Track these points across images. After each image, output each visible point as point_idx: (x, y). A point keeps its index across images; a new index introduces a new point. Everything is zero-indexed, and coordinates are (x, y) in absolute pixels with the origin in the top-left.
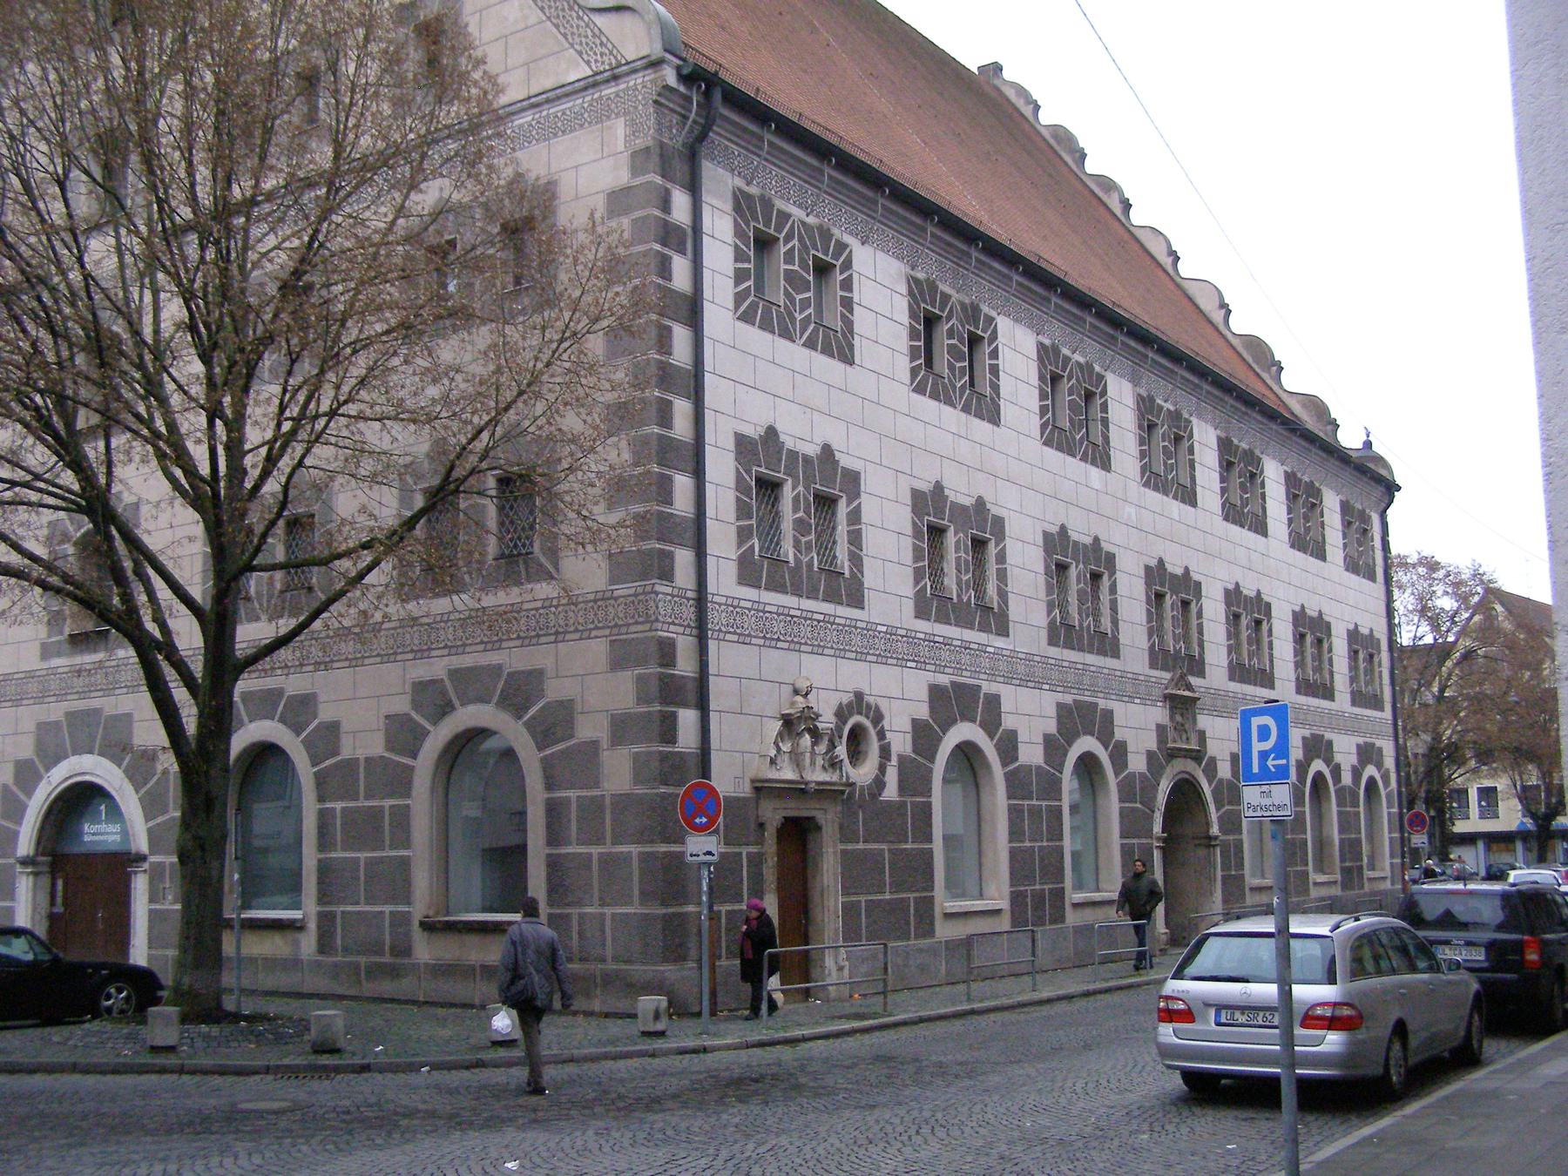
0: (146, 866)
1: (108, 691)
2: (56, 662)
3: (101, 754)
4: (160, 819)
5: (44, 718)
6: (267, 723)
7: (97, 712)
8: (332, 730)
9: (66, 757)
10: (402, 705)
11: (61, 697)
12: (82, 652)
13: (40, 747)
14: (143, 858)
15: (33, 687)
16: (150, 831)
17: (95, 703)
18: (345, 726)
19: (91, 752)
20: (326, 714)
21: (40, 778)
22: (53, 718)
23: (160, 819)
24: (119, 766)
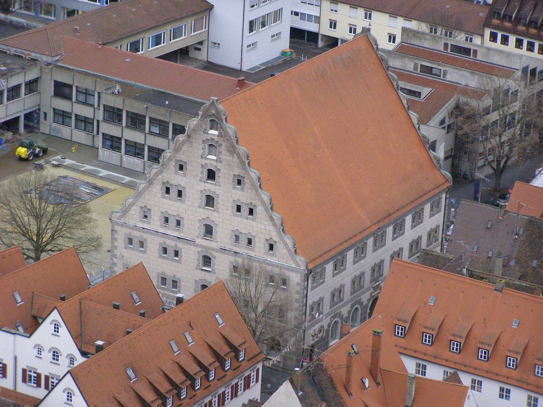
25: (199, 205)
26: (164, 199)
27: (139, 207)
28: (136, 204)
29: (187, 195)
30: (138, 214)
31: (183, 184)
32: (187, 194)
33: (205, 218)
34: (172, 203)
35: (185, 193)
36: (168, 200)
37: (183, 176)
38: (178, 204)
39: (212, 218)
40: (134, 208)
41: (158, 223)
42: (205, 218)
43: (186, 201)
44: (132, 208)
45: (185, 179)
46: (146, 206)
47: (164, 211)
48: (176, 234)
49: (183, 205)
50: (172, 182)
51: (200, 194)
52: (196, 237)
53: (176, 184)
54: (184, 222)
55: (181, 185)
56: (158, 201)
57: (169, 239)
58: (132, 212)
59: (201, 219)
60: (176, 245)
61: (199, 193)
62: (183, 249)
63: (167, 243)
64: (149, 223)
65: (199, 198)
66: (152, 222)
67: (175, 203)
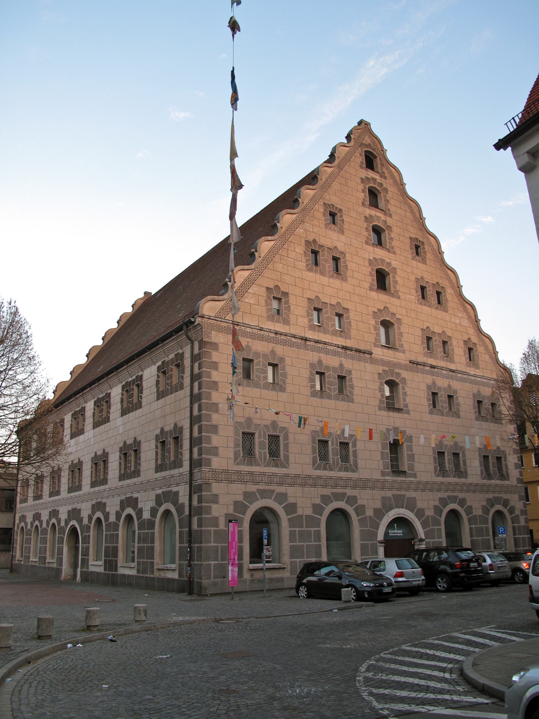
0: (424, 543)
1: (407, 489)
2: (387, 478)
3: (406, 509)
4: (427, 529)
5: (384, 495)
6: (455, 504)
7: (404, 496)
8: (470, 507)
9: (394, 509)
10: (485, 503)
11: (391, 489)
12: (396, 476)
13: (383, 504)
14: (424, 540)
15: (379, 485)
16: (425, 532)
17: (403, 493)
18: (473, 507)
19: (403, 508)
20: (469, 503)
21: (384, 515)
22: (387, 496)
23: (427, 529)
24: (413, 513)
25: (369, 284)
26: (311, 274)
27: (264, 289)
28: (258, 282)
29: (349, 267)
30: (263, 302)
31: (341, 247)
32: (350, 265)
33: (382, 308)
34: (325, 280)
35: (345, 262)
36: (318, 276)
37: (338, 232)
38: (336, 283)
39: (392, 309)
40: (253, 289)
41: (304, 321)
42: (382, 308)
43: (349, 279)
44: (250, 291)
45: (342, 238)
46: (277, 287)
47: (313, 297)
48: (341, 341)
49: (344, 284)
50: (322, 241)
51: (370, 265)
52: (372, 344)
53: (330, 245)
54: (351, 317)
55: (338, 247)
56: (300, 275)
57: (327, 352)
58: (249, 299)
59: (376, 310)
60: (341, 365)
61: (367, 264)
62: (353, 372)
63: (324, 362)
64: (286, 322)
65: (368, 273)
66: (292, 318)
67: (331, 280)
